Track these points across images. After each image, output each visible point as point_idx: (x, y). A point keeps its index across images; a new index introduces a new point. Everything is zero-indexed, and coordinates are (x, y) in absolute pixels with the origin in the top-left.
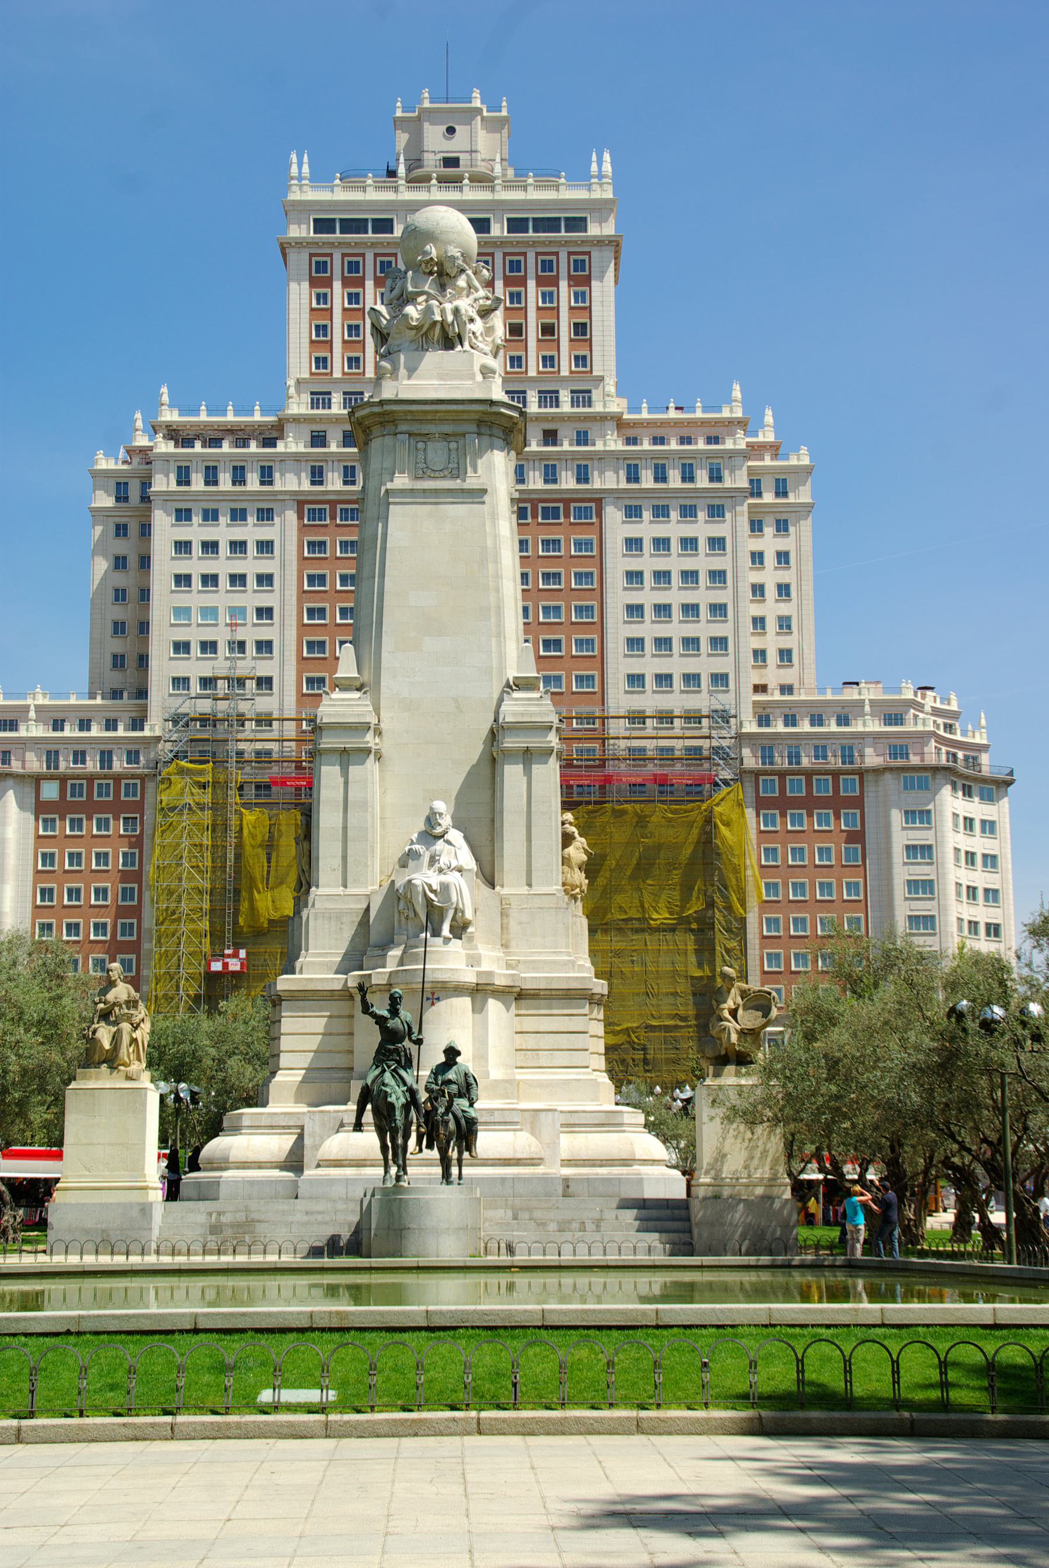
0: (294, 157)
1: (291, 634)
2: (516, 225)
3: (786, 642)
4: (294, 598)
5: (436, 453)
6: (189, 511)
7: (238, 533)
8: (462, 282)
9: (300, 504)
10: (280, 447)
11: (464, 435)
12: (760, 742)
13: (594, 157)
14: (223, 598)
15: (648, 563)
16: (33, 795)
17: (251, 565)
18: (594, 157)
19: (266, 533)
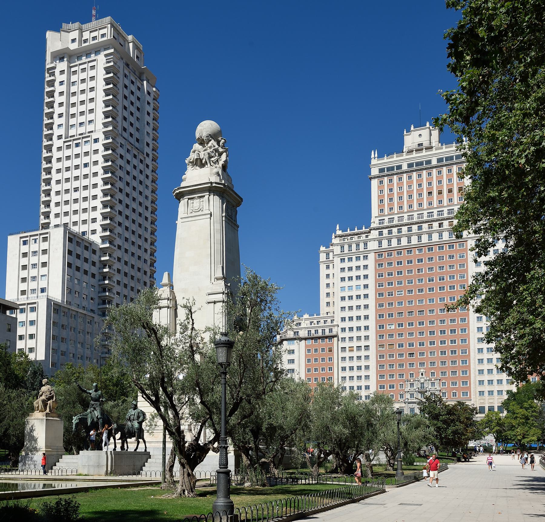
5: (196, 203)
6: (344, 259)
7: (358, 263)
8: (210, 144)
10: (370, 237)
11: (204, 196)
14: (354, 283)
17: (362, 273)
19: (365, 262)
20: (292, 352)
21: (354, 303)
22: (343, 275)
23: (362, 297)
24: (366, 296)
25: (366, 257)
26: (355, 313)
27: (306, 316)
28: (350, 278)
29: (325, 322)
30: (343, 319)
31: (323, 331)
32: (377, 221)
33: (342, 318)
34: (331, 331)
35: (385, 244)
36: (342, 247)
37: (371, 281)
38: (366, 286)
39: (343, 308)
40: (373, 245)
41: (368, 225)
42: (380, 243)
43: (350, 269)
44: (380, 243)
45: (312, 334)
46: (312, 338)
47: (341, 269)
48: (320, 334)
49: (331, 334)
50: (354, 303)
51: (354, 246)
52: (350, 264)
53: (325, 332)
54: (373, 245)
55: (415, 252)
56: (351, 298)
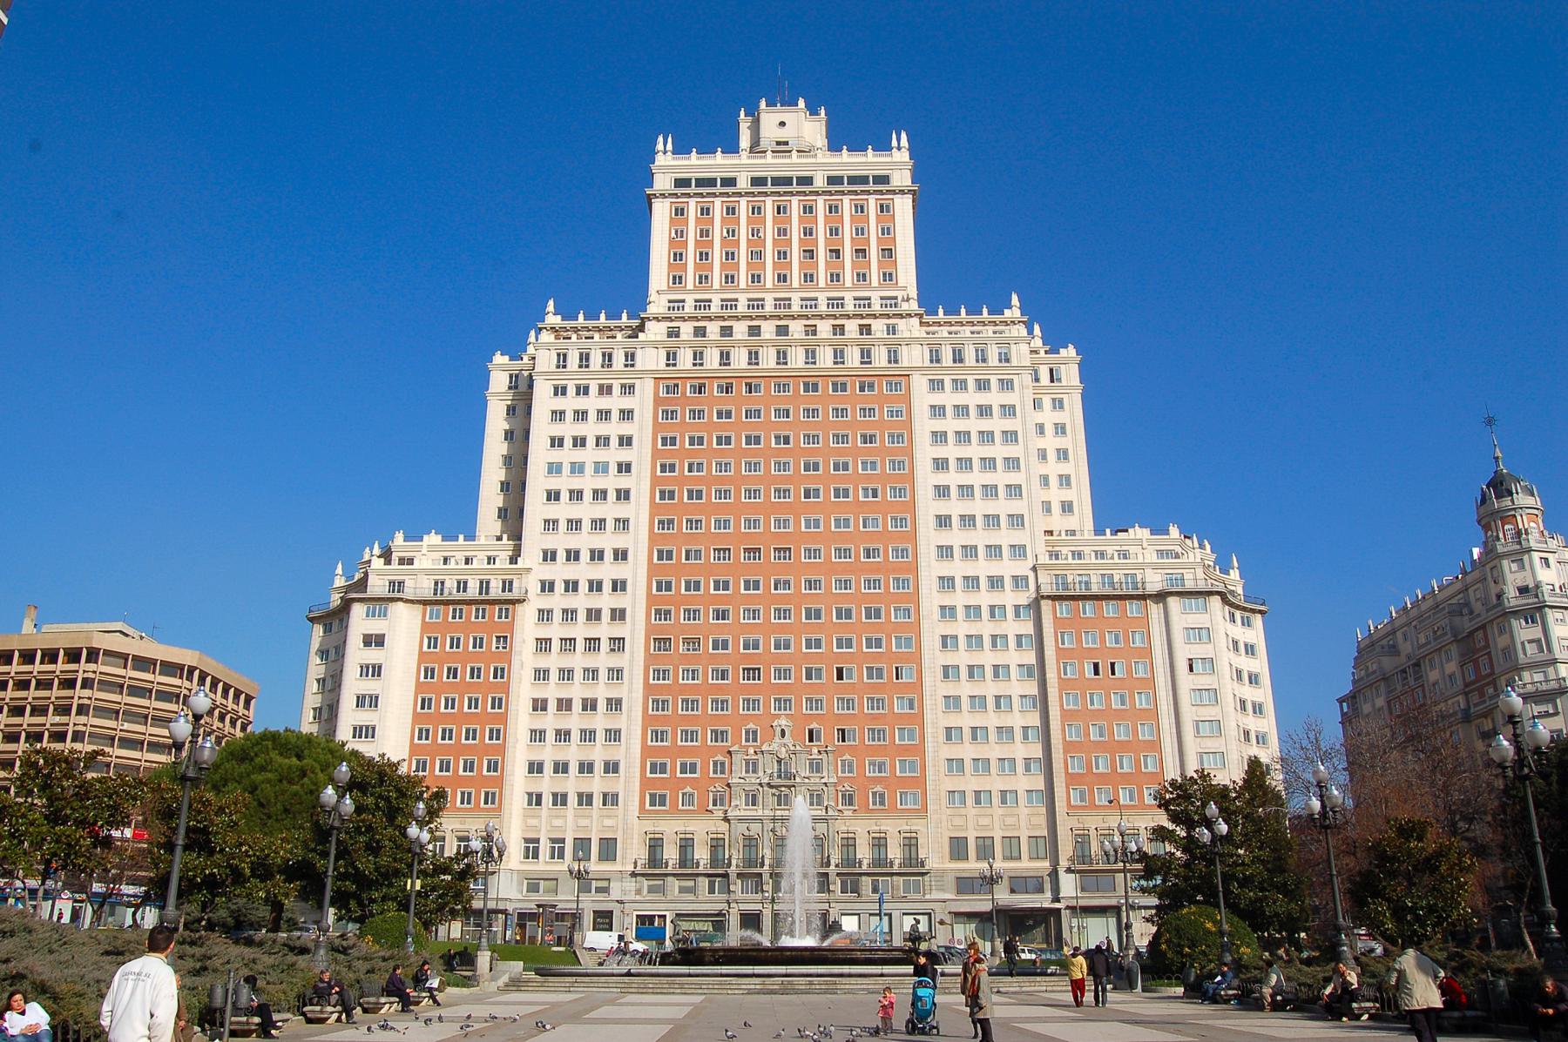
0: (661, 139)
2: (832, 180)
3: (1068, 495)
4: (650, 455)
12: (1055, 572)
13: (894, 136)
14: (589, 455)
16: (420, 617)
17: (614, 429)
18: (894, 136)
19: (627, 403)
21: (586, 511)
22: (557, 430)
24: (623, 495)
25: (628, 389)
26: (585, 541)
27: (433, 539)
28: (580, 442)
29: (491, 560)
30: (549, 556)
31: (485, 586)
32: (664, 299)
33: (545, 553)
34: (507, 585)
35: (685, 359)
36: (562, 359)
37: (641, 455)
38: (625, 468)
40: (651, 359)
41: (643, 301)
42: (671, 357)
43: (581, 415)
44: (671, 357)
45: (446, 591)
46: (447, 603)
47: (554, 412)
48: (473, 591)
49: (507, 595)
50: (586, 511)
51: (596, 360)
52: (581, 403)
53: (487, 588)
54: (651, 359)
55: (768, 389)
56: (576, 495)
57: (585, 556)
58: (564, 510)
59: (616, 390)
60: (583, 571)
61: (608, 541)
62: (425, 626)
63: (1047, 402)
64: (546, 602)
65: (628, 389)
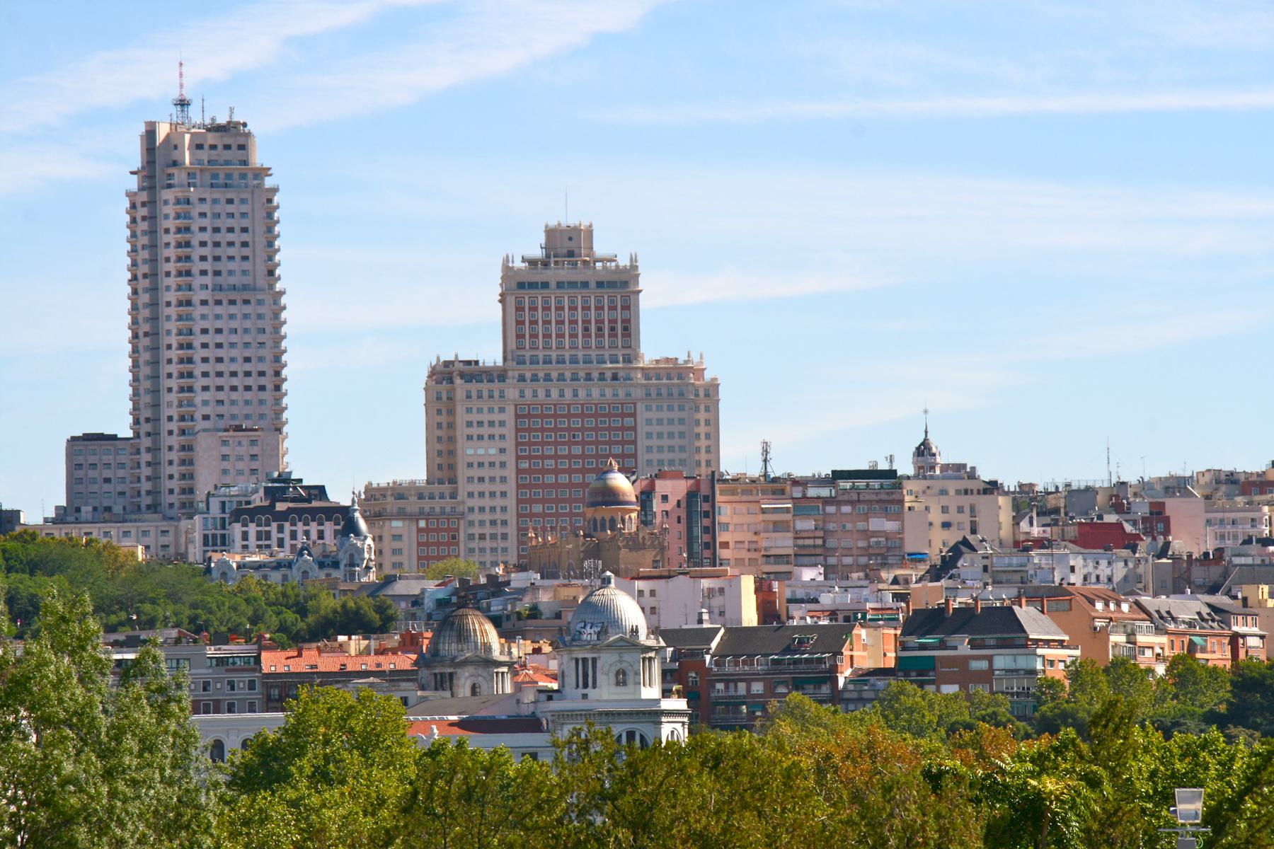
1: (513, 460)
2: (600, 284)
9: (516, 405)
15: (655, 429)
17: (497, 431)
19: (502, 417)
20: (397, 537)
21: (486, 472)
22: (470, 431)
23: (498, 465)
26: (487, 487)
28: (480, 437)
35: (528, 393)
37: (510, 444)
39: (470, 479)
40: (512, 394)
43: (480, 424)
50: (486, 472)
54: (512, 394)
57: (487, 495)
58: (476, 473)
59: (496, 410)
60: (487, 502)
61: (498, 488)
62: (419, 530)
63: (702, 408)
64: (471, 517)
65: (502, 410)
